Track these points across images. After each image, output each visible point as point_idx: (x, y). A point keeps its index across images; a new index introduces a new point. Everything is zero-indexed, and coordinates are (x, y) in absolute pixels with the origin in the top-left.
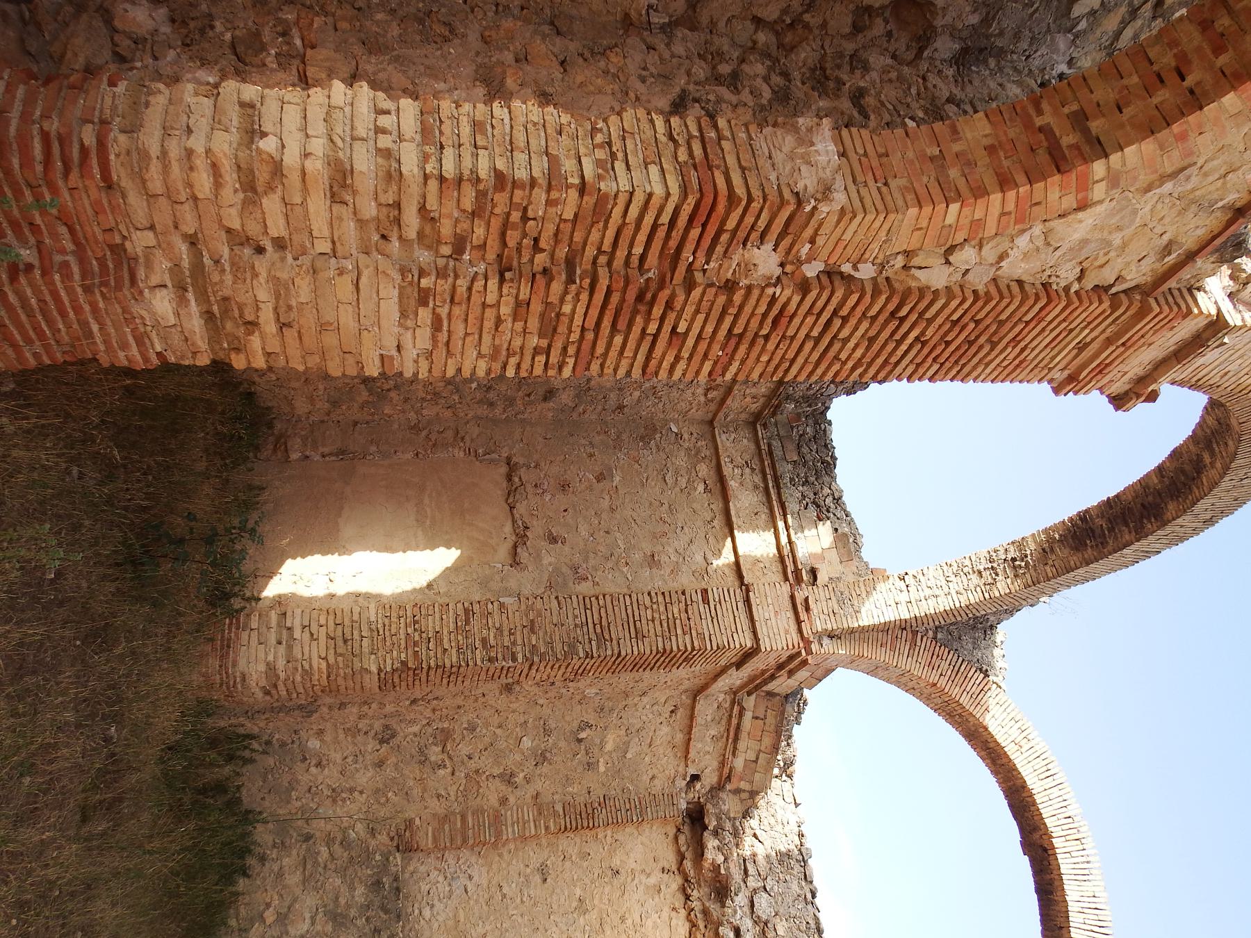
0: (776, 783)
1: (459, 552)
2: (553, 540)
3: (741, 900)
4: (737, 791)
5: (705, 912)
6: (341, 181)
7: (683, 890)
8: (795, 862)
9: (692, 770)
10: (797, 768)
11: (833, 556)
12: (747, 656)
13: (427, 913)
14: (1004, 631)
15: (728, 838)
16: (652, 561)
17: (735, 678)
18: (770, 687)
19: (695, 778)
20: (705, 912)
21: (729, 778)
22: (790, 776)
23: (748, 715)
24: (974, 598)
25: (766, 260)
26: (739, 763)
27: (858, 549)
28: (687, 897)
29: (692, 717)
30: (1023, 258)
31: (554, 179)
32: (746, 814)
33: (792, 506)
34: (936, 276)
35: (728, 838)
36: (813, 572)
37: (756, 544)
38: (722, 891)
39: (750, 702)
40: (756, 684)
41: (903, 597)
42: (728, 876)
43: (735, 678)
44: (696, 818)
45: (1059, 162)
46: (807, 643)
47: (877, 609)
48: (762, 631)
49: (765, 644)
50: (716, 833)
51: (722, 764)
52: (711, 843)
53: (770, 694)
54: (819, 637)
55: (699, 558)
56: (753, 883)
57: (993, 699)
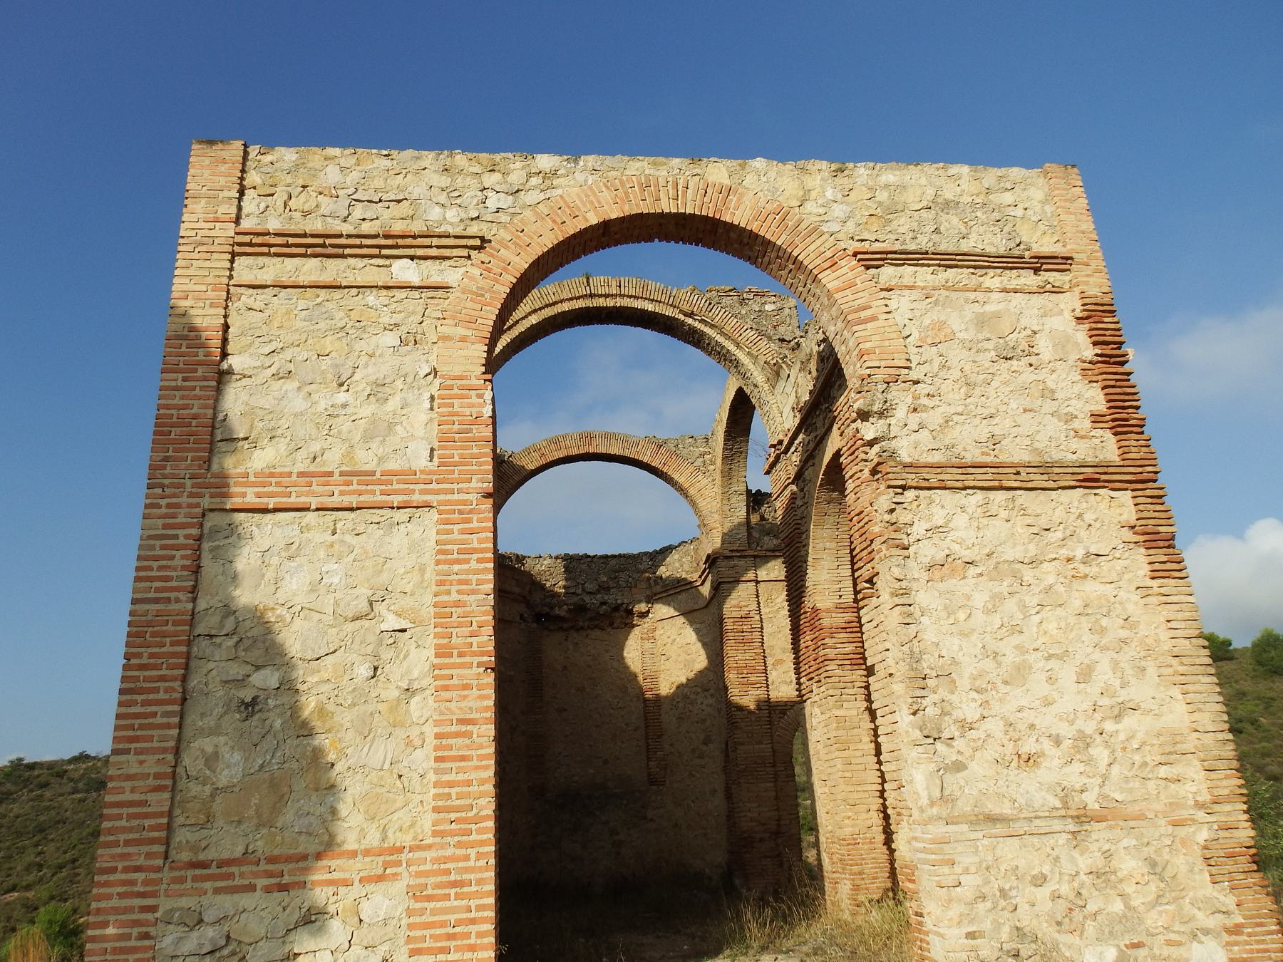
0: (527, 567)
3: (587, 599)
4: (530, 592)
5: (591, 619)
7: (578, 630)
8: (572, 563)
9: (518, 619)
10: (520, 553)
13: (576, 778)
15: (555, 601)
19: (522, 616)
20: (591, 619)
21: (524, 597)
22: (524, 557)
26: (517, 590)
28: (582, 628)
32: (543, 587)
35: (555, 601)
38: (581, 609)
42: (574, 604)
44: (538, 617)
50: (552, 608)
52: (557, 611)
56: (579, 591)
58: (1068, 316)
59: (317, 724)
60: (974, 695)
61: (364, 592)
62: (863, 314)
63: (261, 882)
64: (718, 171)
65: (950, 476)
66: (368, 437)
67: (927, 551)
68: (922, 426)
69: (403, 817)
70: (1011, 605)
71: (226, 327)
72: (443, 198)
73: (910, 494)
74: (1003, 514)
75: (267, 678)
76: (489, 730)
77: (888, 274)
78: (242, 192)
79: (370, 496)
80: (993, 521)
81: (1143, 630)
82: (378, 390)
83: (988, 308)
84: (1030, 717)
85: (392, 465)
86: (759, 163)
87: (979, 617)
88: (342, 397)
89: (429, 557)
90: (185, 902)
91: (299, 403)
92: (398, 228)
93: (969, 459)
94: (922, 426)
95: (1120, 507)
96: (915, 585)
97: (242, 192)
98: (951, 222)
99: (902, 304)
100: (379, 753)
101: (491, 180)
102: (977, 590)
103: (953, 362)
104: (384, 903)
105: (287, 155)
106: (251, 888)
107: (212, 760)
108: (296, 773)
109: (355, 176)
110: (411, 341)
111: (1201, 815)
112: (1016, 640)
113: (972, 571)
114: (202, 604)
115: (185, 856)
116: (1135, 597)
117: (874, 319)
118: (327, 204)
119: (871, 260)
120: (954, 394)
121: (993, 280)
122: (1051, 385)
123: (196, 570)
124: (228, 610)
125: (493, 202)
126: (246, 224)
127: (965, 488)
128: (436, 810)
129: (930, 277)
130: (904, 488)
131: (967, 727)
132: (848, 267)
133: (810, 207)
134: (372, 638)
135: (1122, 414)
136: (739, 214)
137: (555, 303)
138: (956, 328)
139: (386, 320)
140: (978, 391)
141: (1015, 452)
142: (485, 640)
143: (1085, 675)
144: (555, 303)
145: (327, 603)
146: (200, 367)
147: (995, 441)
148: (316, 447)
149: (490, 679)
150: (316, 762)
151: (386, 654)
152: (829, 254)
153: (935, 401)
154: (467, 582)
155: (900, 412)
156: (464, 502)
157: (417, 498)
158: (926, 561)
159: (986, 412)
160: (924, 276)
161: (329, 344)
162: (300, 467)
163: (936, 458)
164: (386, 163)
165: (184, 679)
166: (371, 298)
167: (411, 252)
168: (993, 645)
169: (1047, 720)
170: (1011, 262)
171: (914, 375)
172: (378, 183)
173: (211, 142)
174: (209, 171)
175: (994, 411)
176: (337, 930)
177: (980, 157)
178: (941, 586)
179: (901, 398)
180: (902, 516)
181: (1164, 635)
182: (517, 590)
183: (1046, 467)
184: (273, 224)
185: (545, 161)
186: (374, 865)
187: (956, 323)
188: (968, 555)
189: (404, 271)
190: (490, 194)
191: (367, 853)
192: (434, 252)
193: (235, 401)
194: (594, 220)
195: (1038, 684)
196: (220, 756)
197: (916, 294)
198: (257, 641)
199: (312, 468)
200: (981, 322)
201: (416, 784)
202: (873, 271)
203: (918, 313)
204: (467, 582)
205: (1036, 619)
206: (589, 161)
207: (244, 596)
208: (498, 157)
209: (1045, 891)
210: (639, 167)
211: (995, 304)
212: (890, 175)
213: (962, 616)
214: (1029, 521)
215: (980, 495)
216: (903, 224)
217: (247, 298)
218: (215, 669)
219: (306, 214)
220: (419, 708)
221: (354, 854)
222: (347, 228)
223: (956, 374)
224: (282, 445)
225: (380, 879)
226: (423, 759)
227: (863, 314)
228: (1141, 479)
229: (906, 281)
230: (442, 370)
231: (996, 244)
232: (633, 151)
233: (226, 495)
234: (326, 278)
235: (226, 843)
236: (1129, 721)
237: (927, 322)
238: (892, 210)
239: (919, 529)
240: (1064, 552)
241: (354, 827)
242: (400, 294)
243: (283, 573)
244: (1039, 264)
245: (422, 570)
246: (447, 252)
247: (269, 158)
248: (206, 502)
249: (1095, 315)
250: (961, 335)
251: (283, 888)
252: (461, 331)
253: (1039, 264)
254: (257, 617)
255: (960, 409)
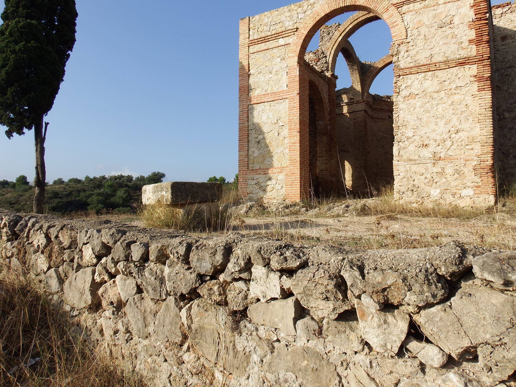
1: (346, 161)
2: (344, 145)
6: (326, 163)
11: (348, 95)
12: (365, 111)
14: (363, 61)
16: (348, 128)
17: (369, 111)
18: (371, 103)
23: (377, 107)
24: (357, 72)
25: (329, 127)
27: (346, 89)
29: (377, 118)
30: (327, 101)
31: (325, 147)
33: (338, 101)
34: (329, 109)
36: (351, 99)
37: (345, 110)
39: (374, 107)
40: (370, 107)
41: (356, 83)
43: (369, 111)
45: (322, 101)
46: (364, 101)
47: (358, 87)
48: (361, 109)
49: (364, 109)
51: (387, 112)
53: (373, 103)
54: (363, 98)
55: (348, 120)
57: (375, 65)
58: (468, 6)
59: (269, 145)
60: (412, 130)
61: (276, 118)
62: (394, 24)
63: (262, 173)
65: (408, 71)
66: (275, 84)
67: (404, 93)
68: (408, 56)
69: (284, 162)
70: (428, 105)
71: (249, 64)
72: (289, 19)
73: (401, 77)
74: (430, 78)
75: (261, 137)
76: (299, 144)
78: (249, 30)
79: (276, 98)
80: (427, 81)
81: (470, 108)
83: (437, 11)
84: (428, 135)
85: (280, 90)
87: (417, 109)
88: (271, 76)
89: (287, 109)
90: (251, 176)
91: (263, 79)
92: (280, 30)
93: (422, 63)
94: (408, 56)
96: (399, 103)
97: (249, 30)
99: (407, 18)
100: (280, 150)
101: (300, 10)
102: (418, 102)
103: (423, 34)
104: (281, 177)
105: (257, 17)
106: (261, 174)
107: (253, 152)
108: (267, 155)
109: (271, 19)
110: (283, 59)
111: (476, 158)
112: (428, 114)
113: (418, 96)
114: (249, 124)
115: (251, 169)
116: (471, 98)
117: (398, 25)
118: (266, 28)
120: (420, 43)
122: (456, 33)
123: (248, 117)
124: (254, 124)
126: (251, 38)
127: (418, 73)
128: (289, 160)
129: (419, 5)
130: (399, 76)
131: (408, 138)
132: (393, 10)
134: (277, 127)
137: (357, 19)
138: (425, 21)
139: (278, 55)
140: (429, 41)
141: (438, 58)
142: (298, 126)
143: (447, 123)
144: (357, 19)
145: (270, 121)
146: (245, 74)
147: (432, 56)
148: (266, 88)
149: (299, 134)
150: (269, 152)
151: (280, 131)
152: (386, 7)
153: (414, 47)
154: (294, 114)
155: (402, 53)
156: (293, 96)
157: (284, 97)
158: (403, 96)
159: (430, 47)
161: (268, 63)
162: (263, 93)
163: (412, 65)
164: (277, 13)
165: (248, 138)
166: (275, 50)
167: (282, 36)
168: (420, 116)
169: (433, 136)
171: (408, 40)
172: (275, 19)
173: (243, 19)
174: (243, 27)
175: (433, 46)
176: (273, 181)
178: (407, 102)
179: (403, 48)
180: (399, 84)
181: (478, 108)
182: (387, 108)
184: (256, 37)
186: (279, 170)
187: (425, 20)
188: (416, 92)
189: (281, 41)
190: (299, 14)
191: (278, 168)
192: (287, 35)
193: (252, 81)
194: (323, 15)
195: (433, 126)
196: (255, 152)
197: (413, 12)
198: (259, 130)
199: (266, 93)
201: (286, 155)
202: (400, 8)
203: (412, 19)
204: (294, 114)
205: (435, 108)
207: (256, 120)
208: (301, 3)
209: (424, 176)
213: (412, 109)
214: (438, 79)
215: (423, 74)
217: (252, 56)
218: (253, 135)
219: (261, 32)
220: (286, 141)
221: (276, 168)
222: (269, 34)
223: (422, 36)
224: (260, 89)
225: (280, 173)
226: (287, 151)
227: (394, 24)
229: (411, 9)
230: (289, 65)
233: (251, 101)
234: (266, 48)
235: (257, 167)
236: (460, 134)
237: (415, 21)
239: (403, 87)
240: (450, 87)
241: (276, 163)
242: (280, 48)
243: (262, 116)
245: (286, 112)
246: (289, 34)
247: (254, 19)
248: (248, 103)
250: (426, 23)
251: (265, 174)
252: (293, 54)
254: (258, 124)
255: (422, 48)
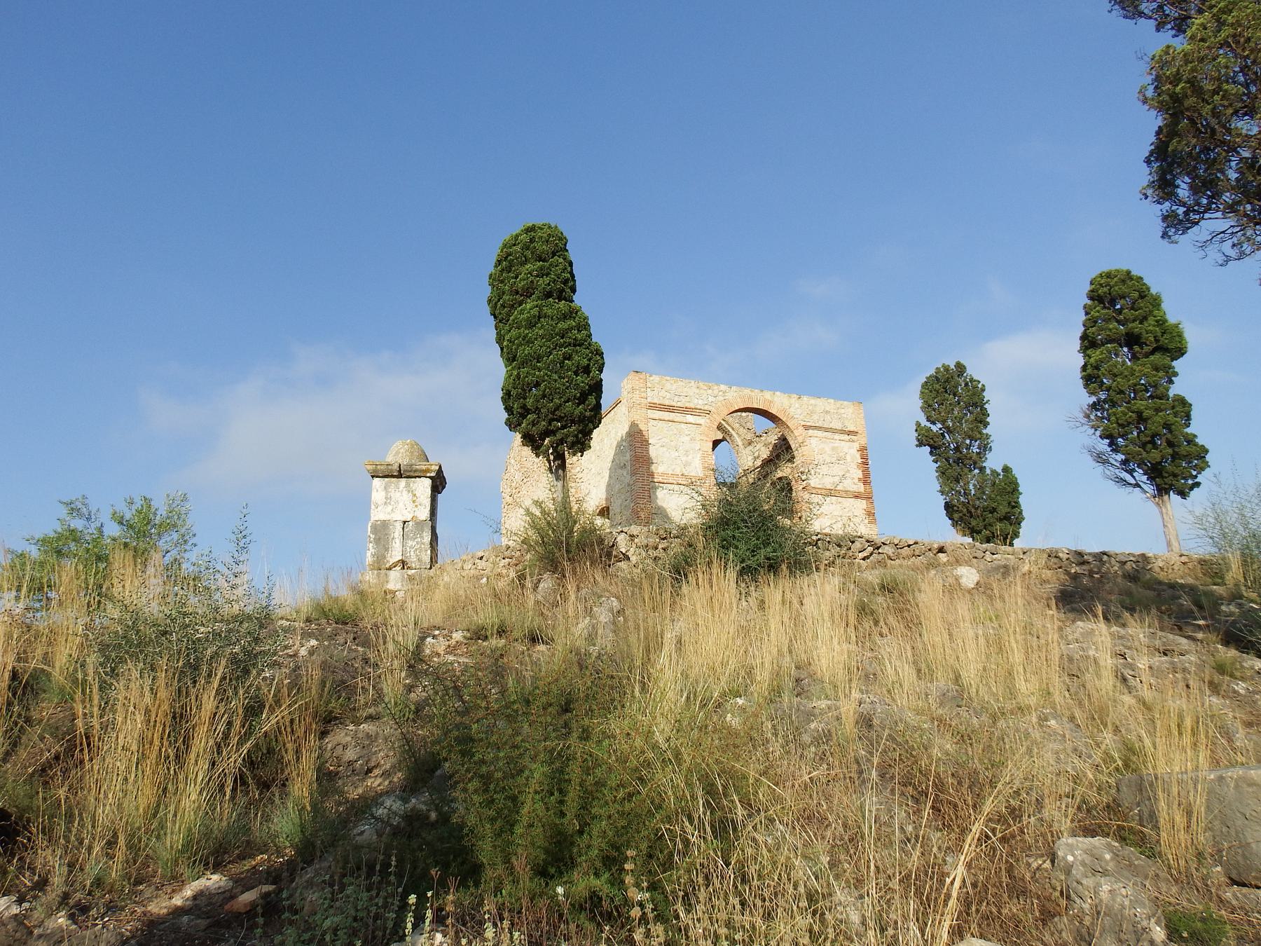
64: (768, 395)
77: (810, 432)
82: (687, 453)
86: (778, 393)
95: (862, 504)
98: (828, 417)
99: (813, 441)
119: (807, 428)
121: (837, 436)
125: (711, 399)
133: (792, 410)
135: (866, 480)
136: (773, 411)
160: (820, 433)
170: (843, 432)
177: (836, 398)
183: (846, 491)
185: (723, 387)
189: (690, 418)
200: (833, 449)
206: (734, 388)
210: (747, 391)
211: (837, 444)
212: (813, 401)
216: (815, 417)
228: (869, 498)
231: (838, 426)
232: (746, 386)
238: (812, 413)
244: (850, 433)
249: (863, 449)
253: (850, 433)
